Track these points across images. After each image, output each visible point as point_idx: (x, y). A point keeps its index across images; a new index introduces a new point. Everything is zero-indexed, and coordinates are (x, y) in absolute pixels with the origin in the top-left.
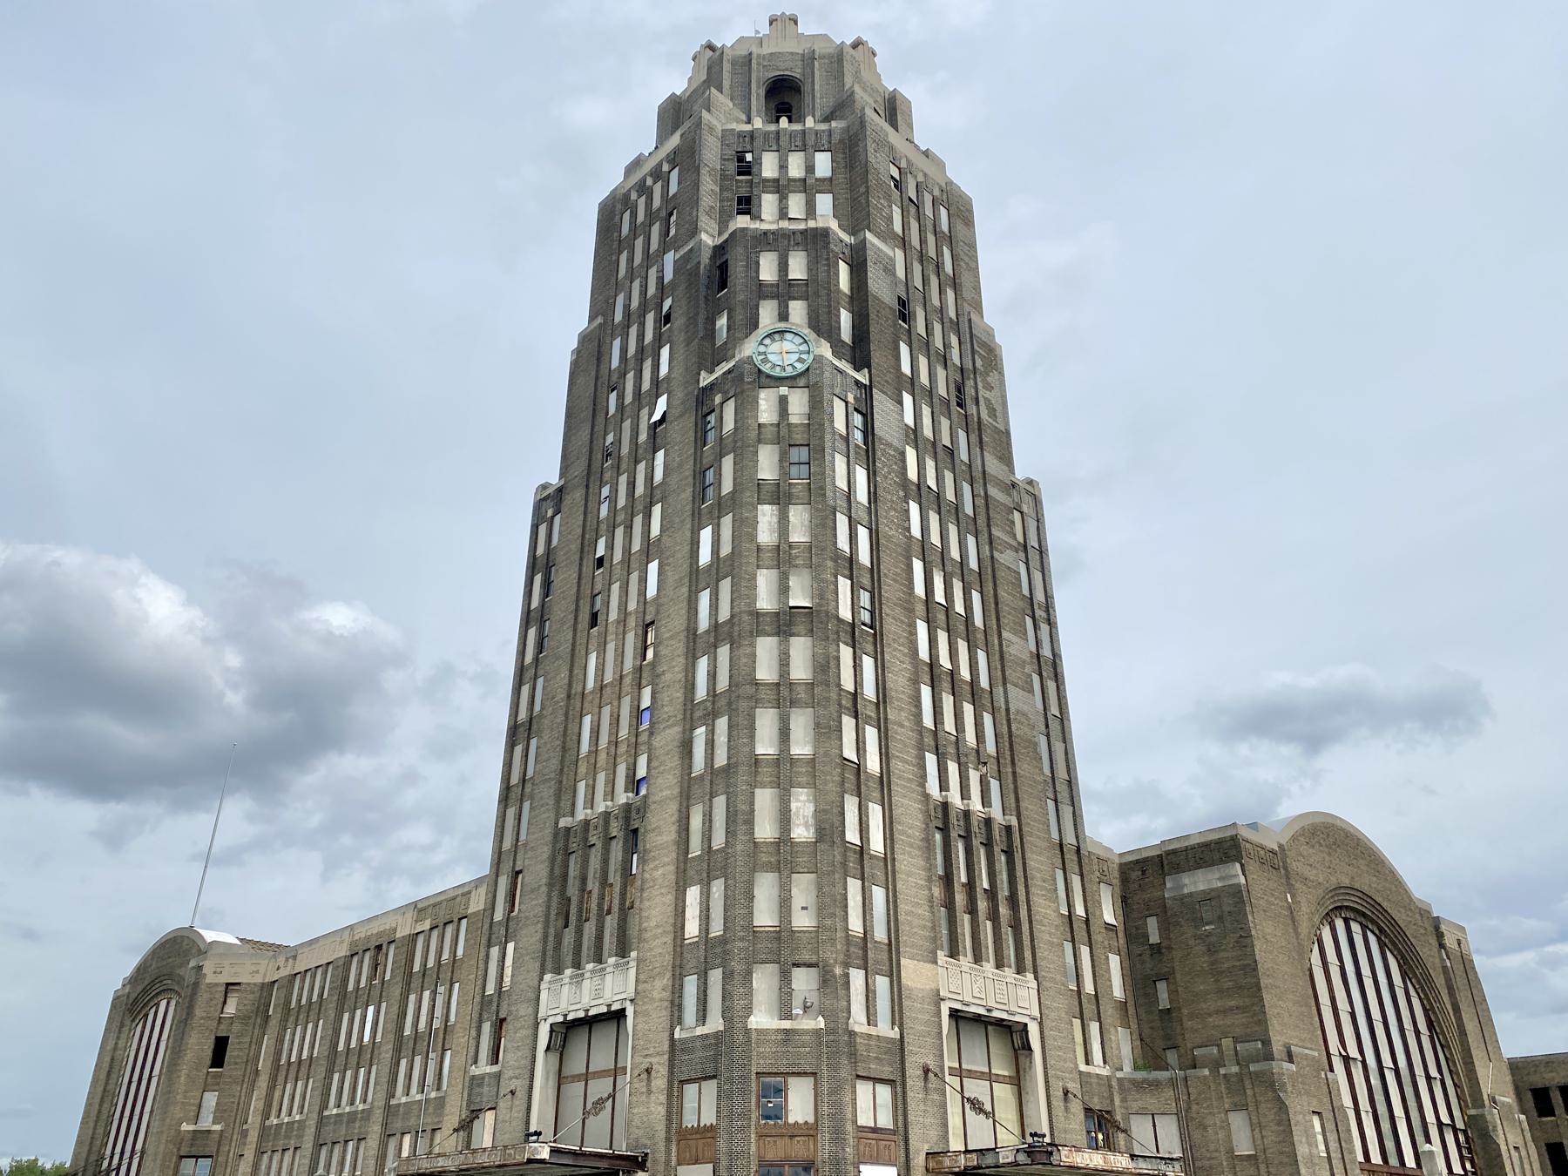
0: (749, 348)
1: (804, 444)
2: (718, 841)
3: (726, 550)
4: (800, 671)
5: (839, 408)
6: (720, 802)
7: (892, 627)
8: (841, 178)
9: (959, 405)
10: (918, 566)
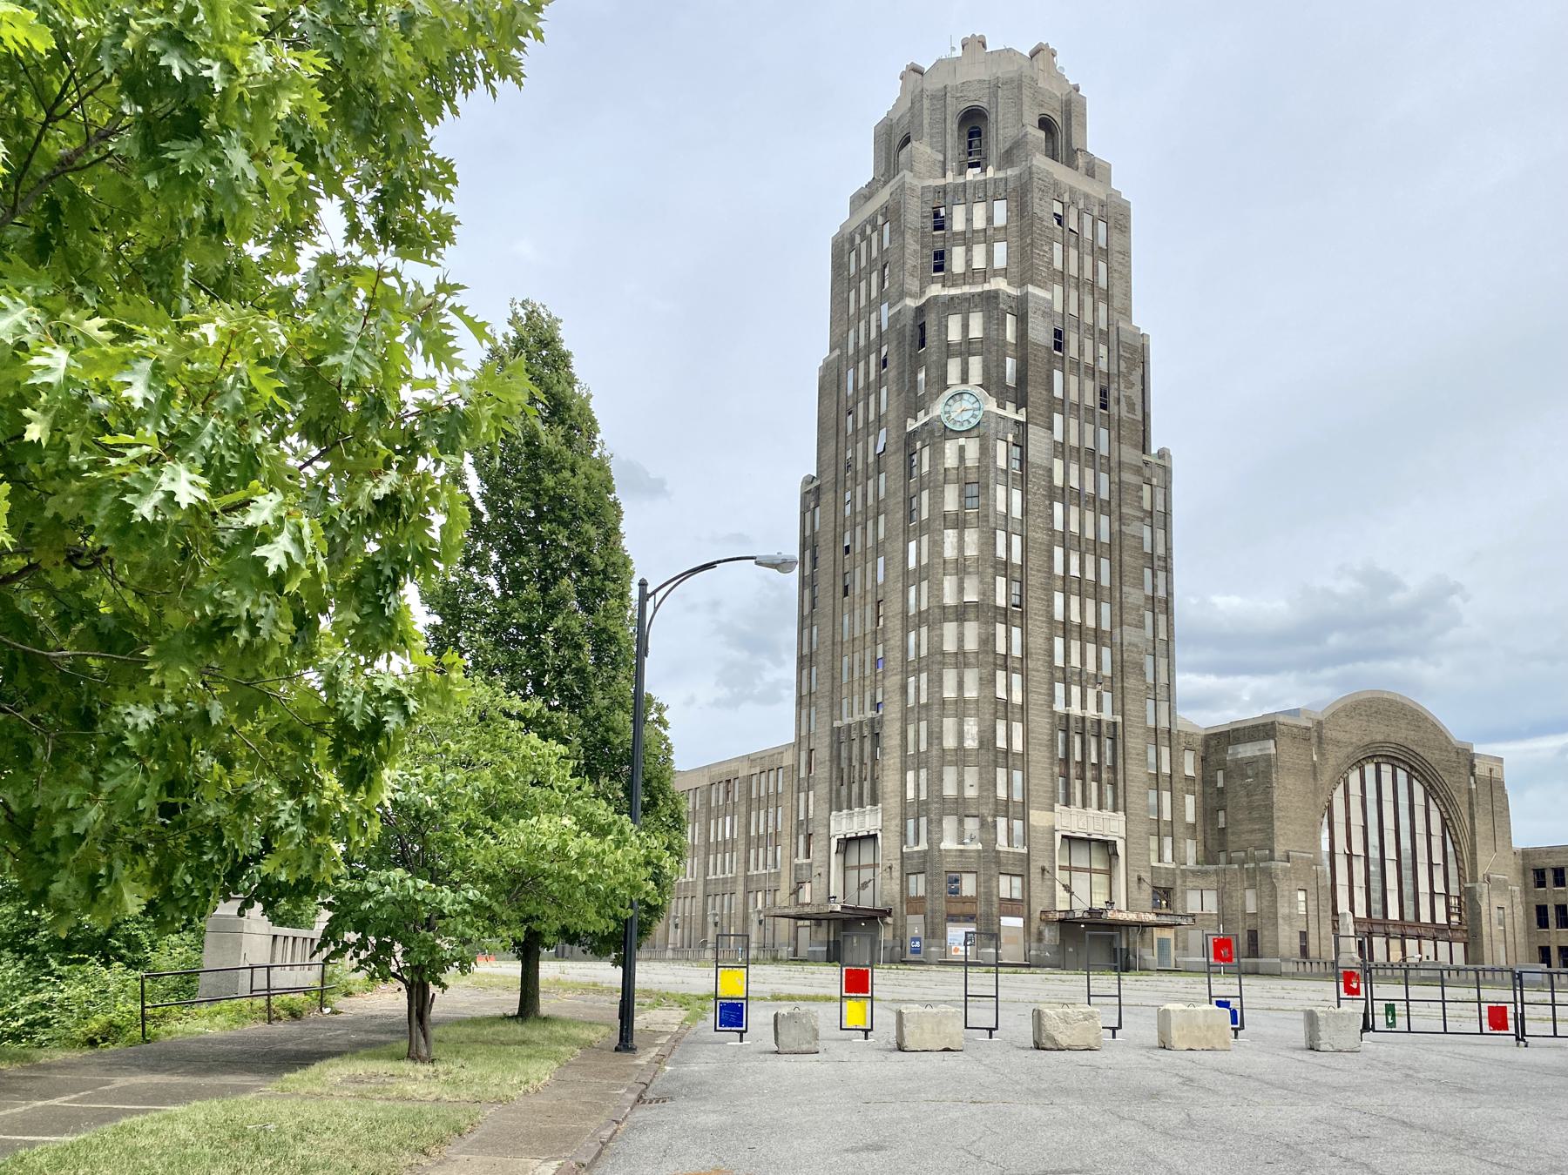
0: (938, 409)
1: (975, 483)
2: (923, 747)
3: (924, 561)
4: (971, 645)
5: (1001, 447)
6: (923, 725)
7: (1034, 605)
8: (1013, 228)
9: (1104, 406)
10: (1058, 552)
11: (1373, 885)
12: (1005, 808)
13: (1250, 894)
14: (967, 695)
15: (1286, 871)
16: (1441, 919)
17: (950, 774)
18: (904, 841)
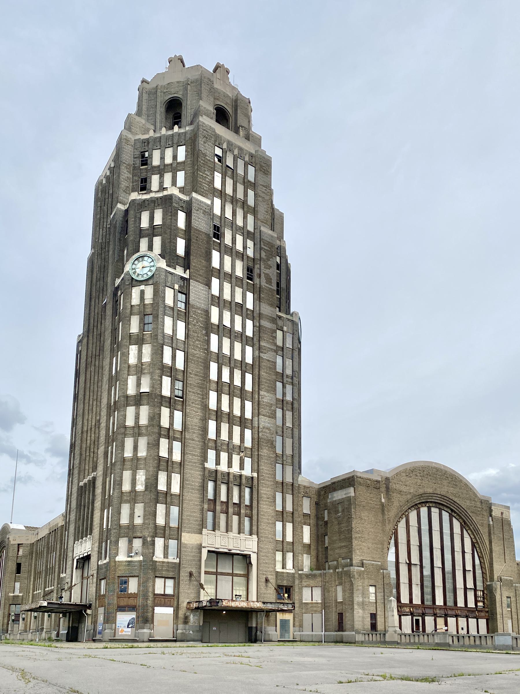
4: (144, 421)
11: (425, 583)
12: (164, 532)
13: (339, 589)
14: (140, 454)
15: (360, 573)
16: (471, 604)
17: (125, 509)
18: (99, 558)
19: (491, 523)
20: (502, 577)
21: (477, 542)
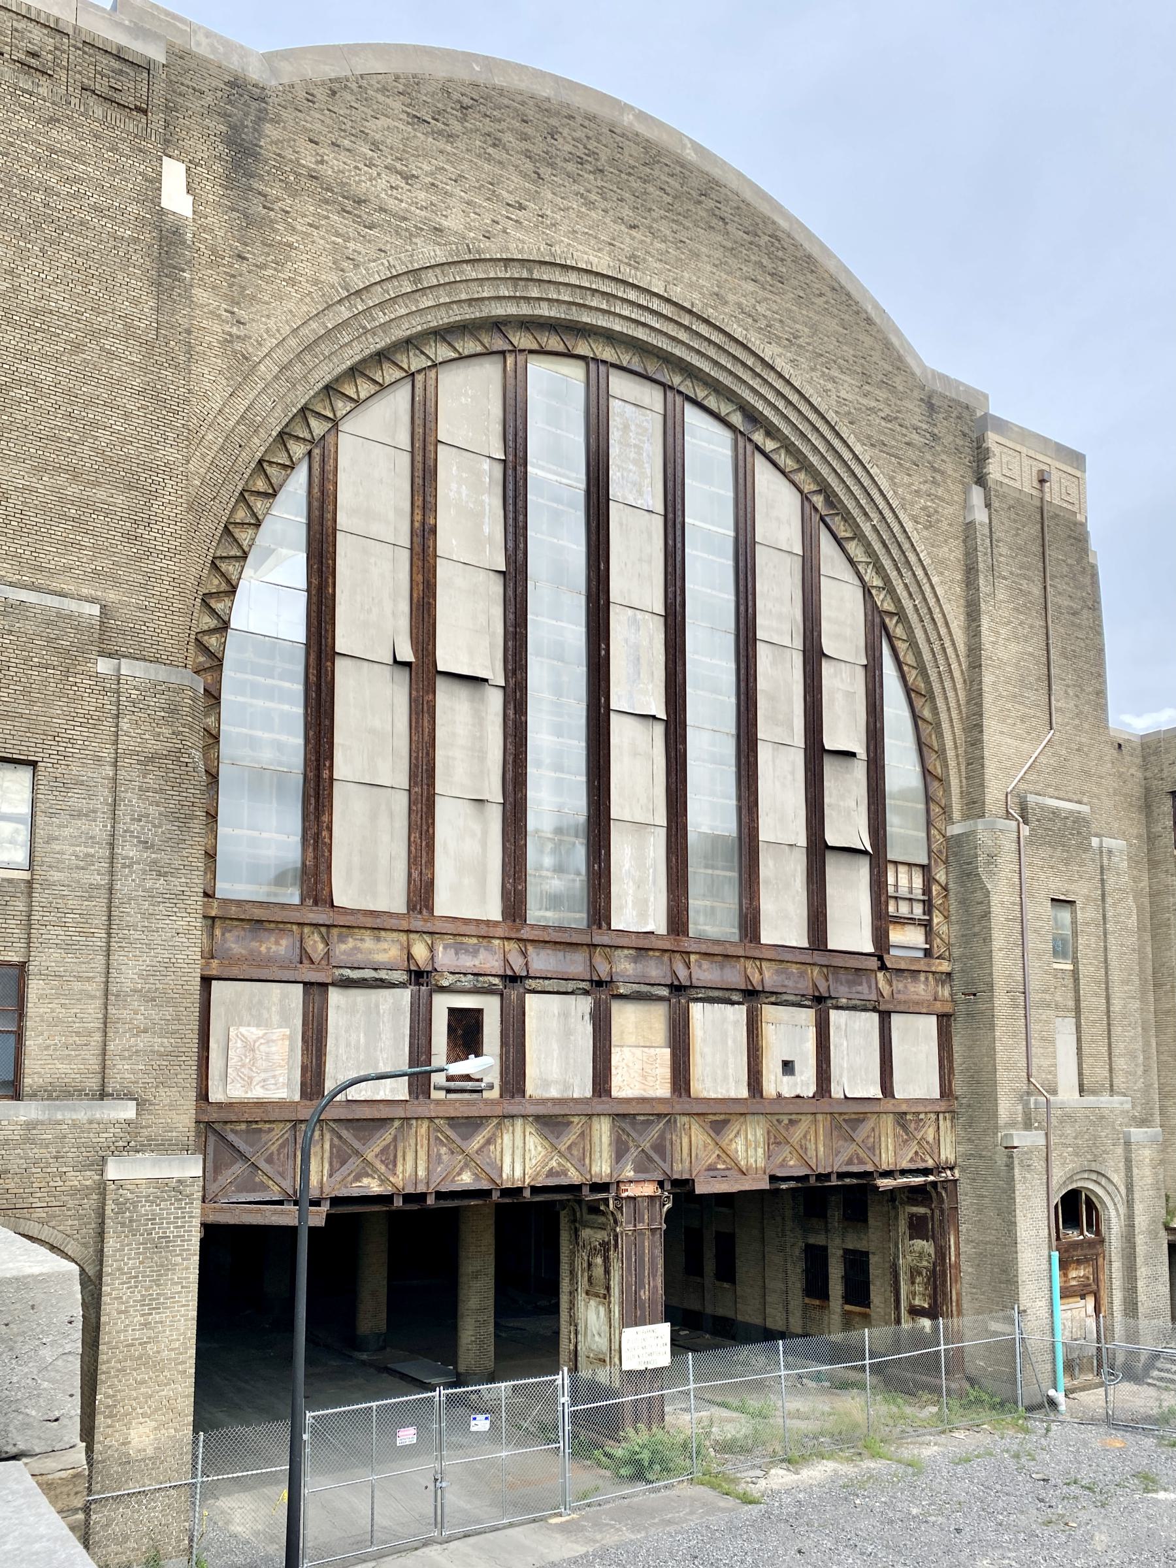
16: (851, 931)
19: (980, 515)
20: (1031, 799)
21: (901, 615)
